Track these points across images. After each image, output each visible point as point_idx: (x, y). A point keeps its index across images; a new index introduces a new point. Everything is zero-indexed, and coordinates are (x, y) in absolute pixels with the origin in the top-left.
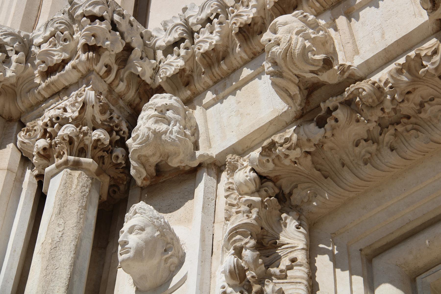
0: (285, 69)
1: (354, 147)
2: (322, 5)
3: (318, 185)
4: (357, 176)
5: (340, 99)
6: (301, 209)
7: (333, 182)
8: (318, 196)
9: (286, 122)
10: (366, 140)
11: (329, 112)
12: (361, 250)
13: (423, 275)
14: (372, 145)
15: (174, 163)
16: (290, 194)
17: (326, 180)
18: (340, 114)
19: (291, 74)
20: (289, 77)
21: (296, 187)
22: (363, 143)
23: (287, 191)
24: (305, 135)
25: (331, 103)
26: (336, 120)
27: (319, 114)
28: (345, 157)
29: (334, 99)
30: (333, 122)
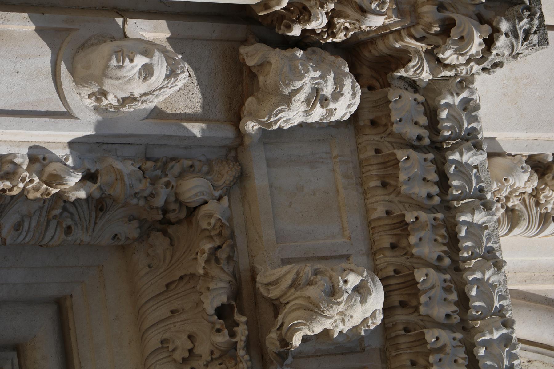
0: (298, 293)
1: (189, 333)
2: (392, 338)
3: (163, 272)
4: (152, 326)
5: (241, 345)
6: (143, 241)
7: (157, 293)
8: (148, 269)
9: (254, 256)
10: (191, 351)
11: (232, 326)
12: (71, 296)
13: (16, 361)
14: (182, 356)
15: (250, 101)
16: (165, 233)
17: (165, 283)
18: (222, 339)
19: (292, 298)
20: (288, 295)
21: (172, 245)
22: (189, 345)
23: (171, 230)
24: (215, 287)
25: (242, 332)
26: (219, 331)
27: (236, 311)
28: (183, 317)
29: (244, 338)
30: (218, 326)
